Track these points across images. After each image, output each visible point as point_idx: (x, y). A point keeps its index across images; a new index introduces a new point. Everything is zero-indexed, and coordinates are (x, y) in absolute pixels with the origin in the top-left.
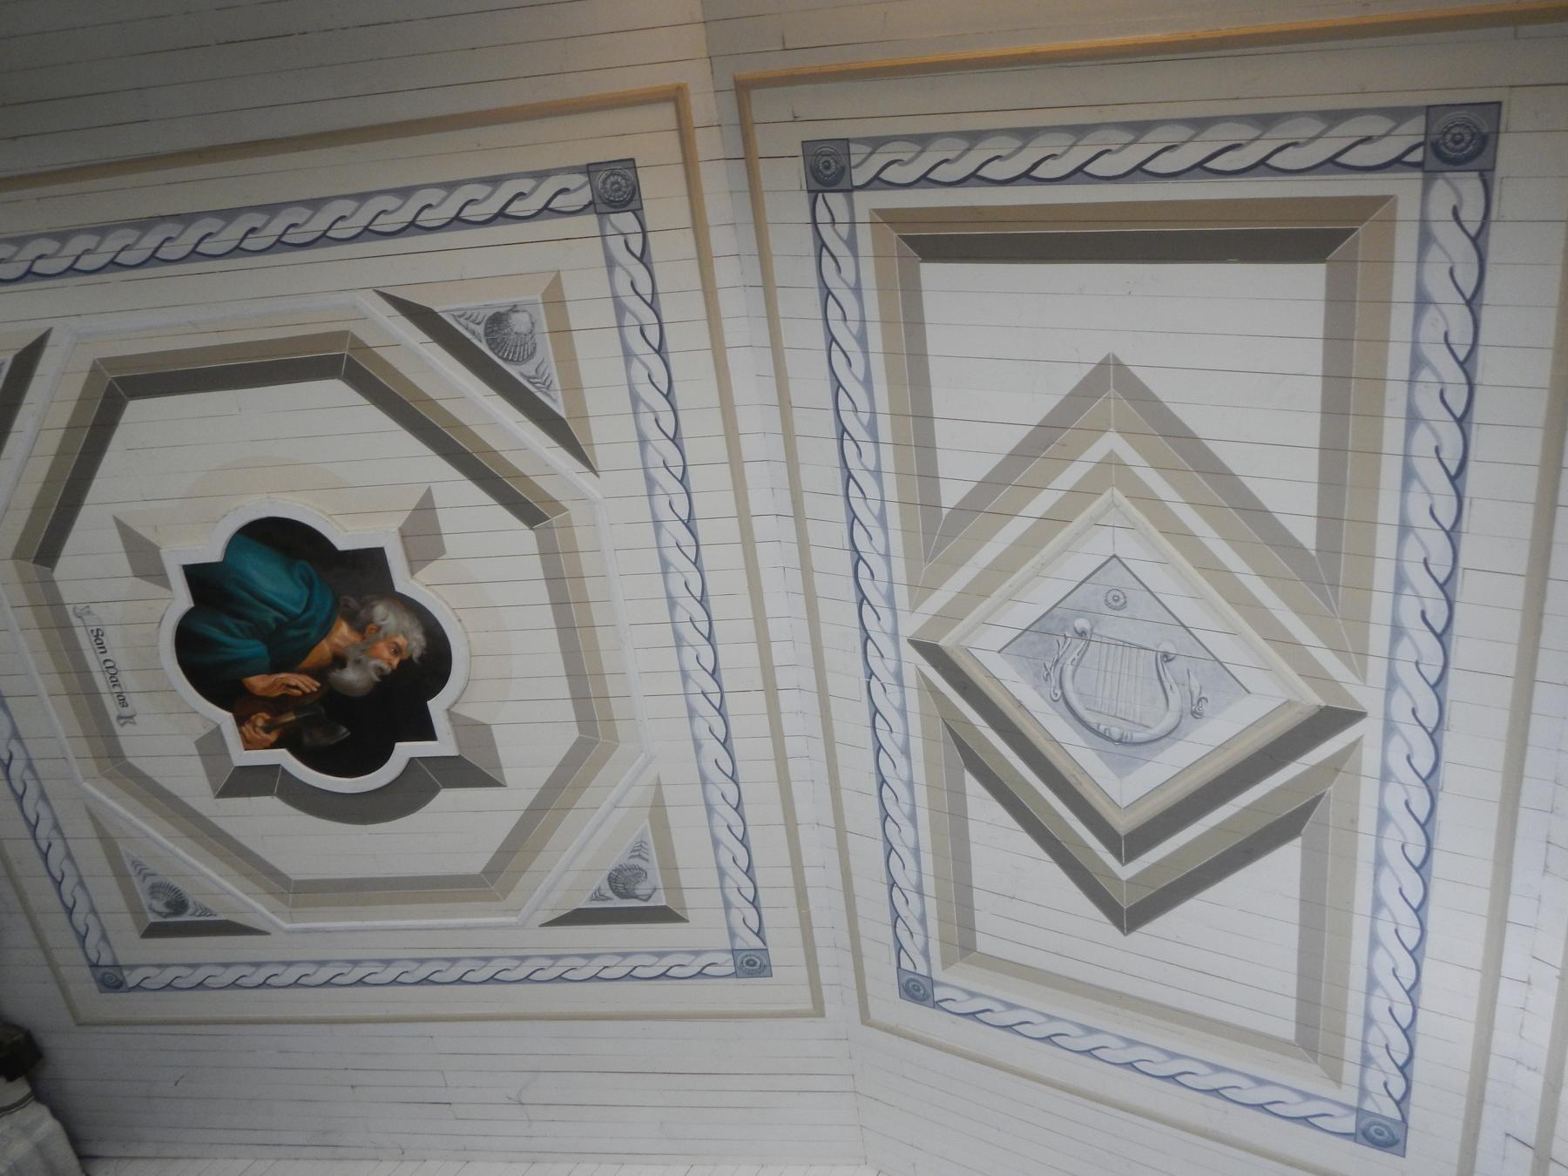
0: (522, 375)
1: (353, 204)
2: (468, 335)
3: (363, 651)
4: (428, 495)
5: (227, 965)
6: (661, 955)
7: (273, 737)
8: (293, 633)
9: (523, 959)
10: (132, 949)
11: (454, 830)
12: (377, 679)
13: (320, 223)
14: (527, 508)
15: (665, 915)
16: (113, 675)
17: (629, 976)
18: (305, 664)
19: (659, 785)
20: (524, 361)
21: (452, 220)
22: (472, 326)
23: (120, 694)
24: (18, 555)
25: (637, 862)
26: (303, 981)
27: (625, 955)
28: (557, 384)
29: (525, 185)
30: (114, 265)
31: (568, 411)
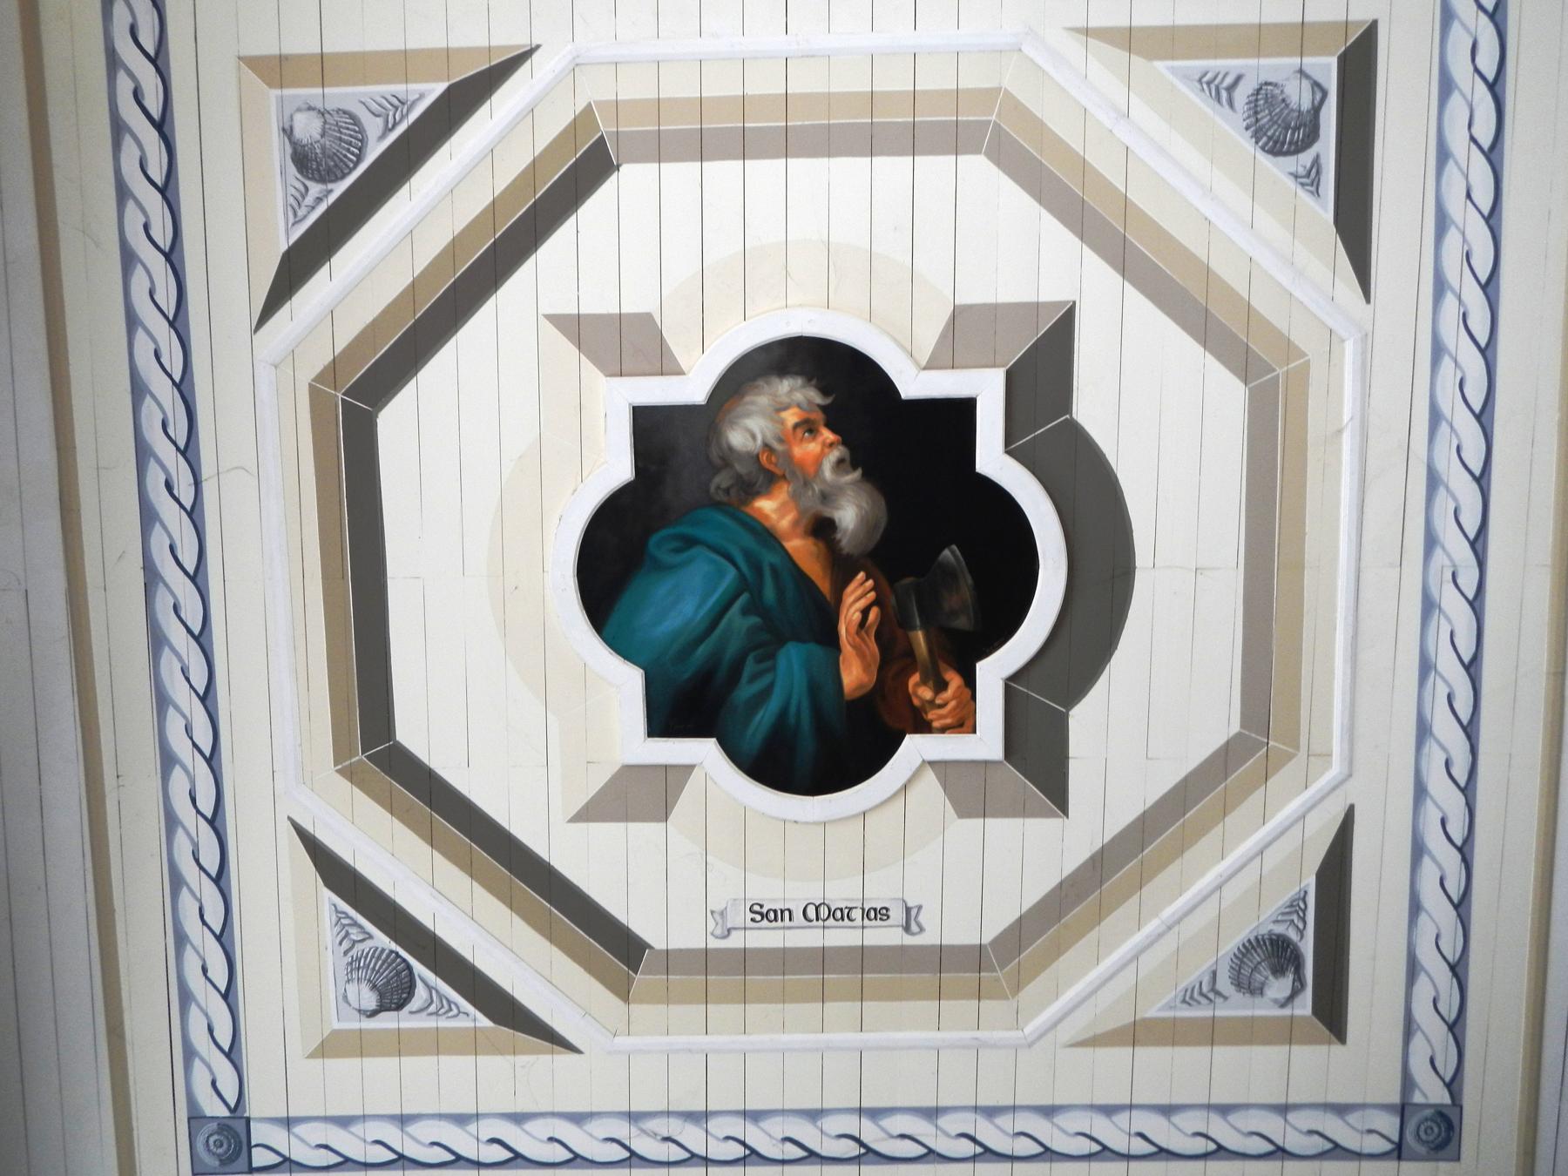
0: (382, 137)
1: (140, 335)
2: (322, 208)
3: (806, 484)
4: (557, 320)
5: (1415, 907)
6: (1446, 86)
7: (955, 681)
8: (769, 593)
9: (1438, 350)
10: (1364, 1067)
11: (1154, 409)
12: (857, 474)
13: (162, 388)
14: (583, 170)
15: (1359, 60)
16: (832, 914)
17: (1493, 154)
18: (824, 585)
19: (1087, 32)
20: (362, 131)
21: (165, 197)
22: (309, 200)
23: (866, 914)
24: (624, 994)
25: (1242, 95)
26: (1461, 775)
27: (1443, 155)
28: (399, 88)
29: (124, 86)
30: (207, 697)
31: (438, 79)
